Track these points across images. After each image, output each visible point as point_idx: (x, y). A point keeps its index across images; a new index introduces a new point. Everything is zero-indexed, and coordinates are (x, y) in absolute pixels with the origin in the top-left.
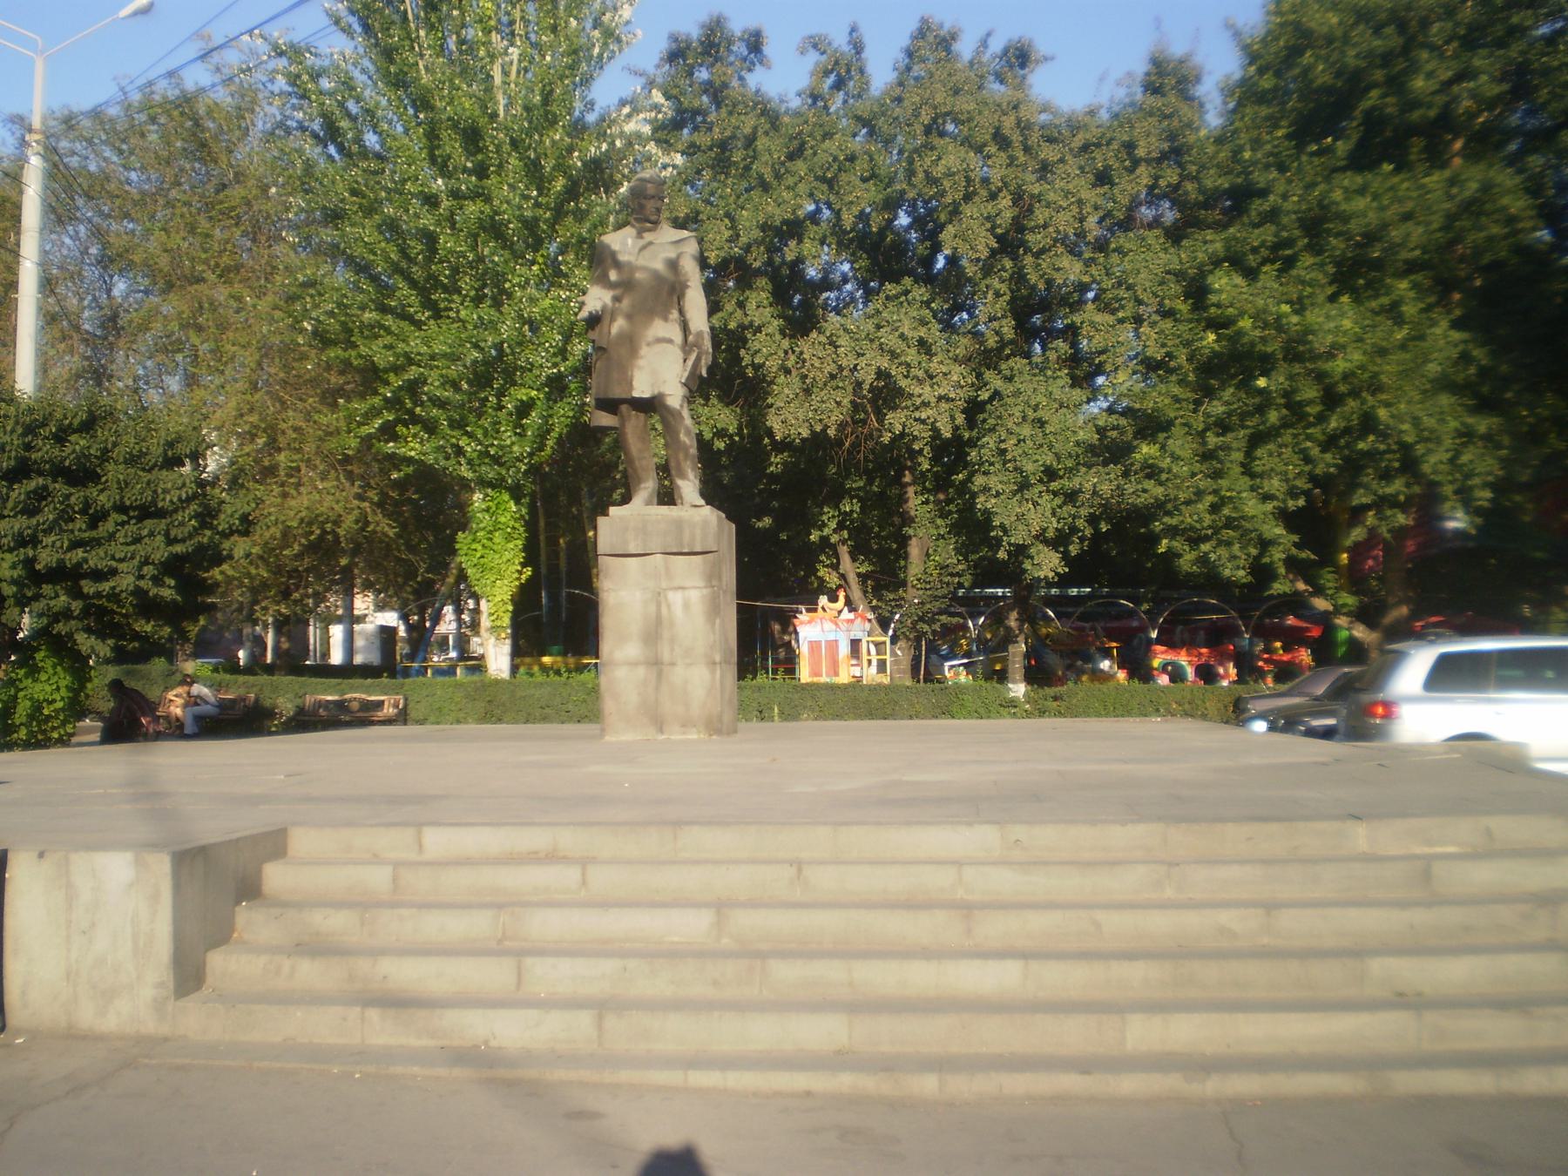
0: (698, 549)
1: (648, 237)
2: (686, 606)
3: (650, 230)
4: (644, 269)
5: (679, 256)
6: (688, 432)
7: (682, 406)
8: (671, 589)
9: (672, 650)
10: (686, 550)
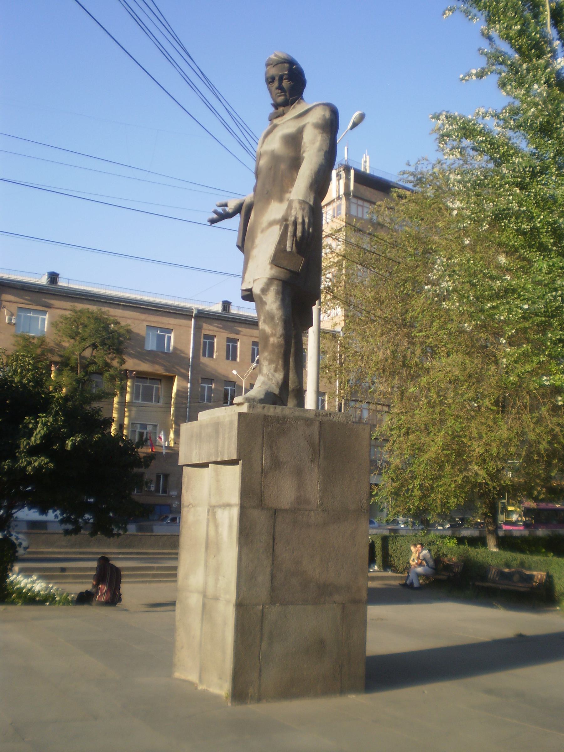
0: (226, 458)
1: (276, 121)
2: (230, 526)
3: (283, 114)
4: (266, 153)
5: (300, 132)
6: (270, 318)
7: (264, 291)
8: (220, 506)
9: (217, 580)
10: (219, 459)
